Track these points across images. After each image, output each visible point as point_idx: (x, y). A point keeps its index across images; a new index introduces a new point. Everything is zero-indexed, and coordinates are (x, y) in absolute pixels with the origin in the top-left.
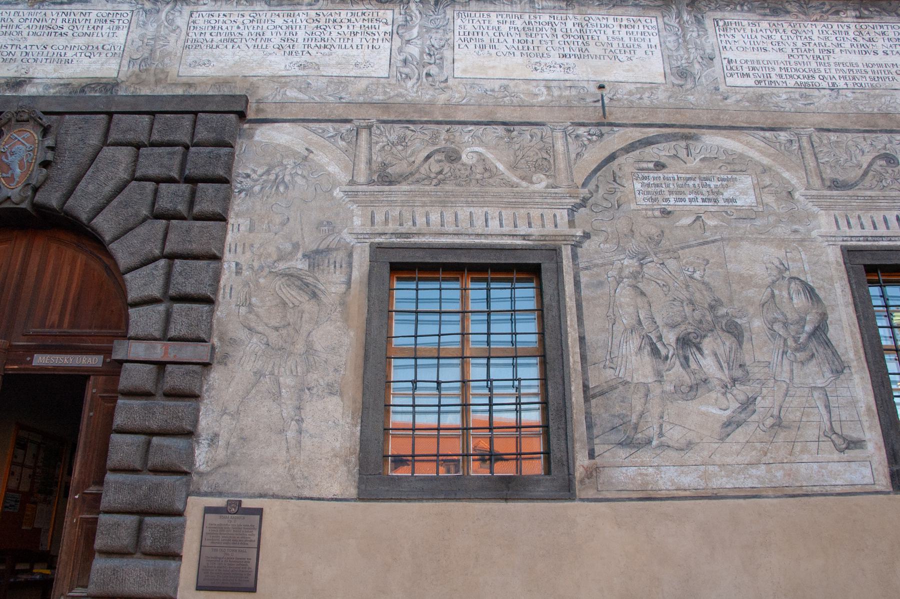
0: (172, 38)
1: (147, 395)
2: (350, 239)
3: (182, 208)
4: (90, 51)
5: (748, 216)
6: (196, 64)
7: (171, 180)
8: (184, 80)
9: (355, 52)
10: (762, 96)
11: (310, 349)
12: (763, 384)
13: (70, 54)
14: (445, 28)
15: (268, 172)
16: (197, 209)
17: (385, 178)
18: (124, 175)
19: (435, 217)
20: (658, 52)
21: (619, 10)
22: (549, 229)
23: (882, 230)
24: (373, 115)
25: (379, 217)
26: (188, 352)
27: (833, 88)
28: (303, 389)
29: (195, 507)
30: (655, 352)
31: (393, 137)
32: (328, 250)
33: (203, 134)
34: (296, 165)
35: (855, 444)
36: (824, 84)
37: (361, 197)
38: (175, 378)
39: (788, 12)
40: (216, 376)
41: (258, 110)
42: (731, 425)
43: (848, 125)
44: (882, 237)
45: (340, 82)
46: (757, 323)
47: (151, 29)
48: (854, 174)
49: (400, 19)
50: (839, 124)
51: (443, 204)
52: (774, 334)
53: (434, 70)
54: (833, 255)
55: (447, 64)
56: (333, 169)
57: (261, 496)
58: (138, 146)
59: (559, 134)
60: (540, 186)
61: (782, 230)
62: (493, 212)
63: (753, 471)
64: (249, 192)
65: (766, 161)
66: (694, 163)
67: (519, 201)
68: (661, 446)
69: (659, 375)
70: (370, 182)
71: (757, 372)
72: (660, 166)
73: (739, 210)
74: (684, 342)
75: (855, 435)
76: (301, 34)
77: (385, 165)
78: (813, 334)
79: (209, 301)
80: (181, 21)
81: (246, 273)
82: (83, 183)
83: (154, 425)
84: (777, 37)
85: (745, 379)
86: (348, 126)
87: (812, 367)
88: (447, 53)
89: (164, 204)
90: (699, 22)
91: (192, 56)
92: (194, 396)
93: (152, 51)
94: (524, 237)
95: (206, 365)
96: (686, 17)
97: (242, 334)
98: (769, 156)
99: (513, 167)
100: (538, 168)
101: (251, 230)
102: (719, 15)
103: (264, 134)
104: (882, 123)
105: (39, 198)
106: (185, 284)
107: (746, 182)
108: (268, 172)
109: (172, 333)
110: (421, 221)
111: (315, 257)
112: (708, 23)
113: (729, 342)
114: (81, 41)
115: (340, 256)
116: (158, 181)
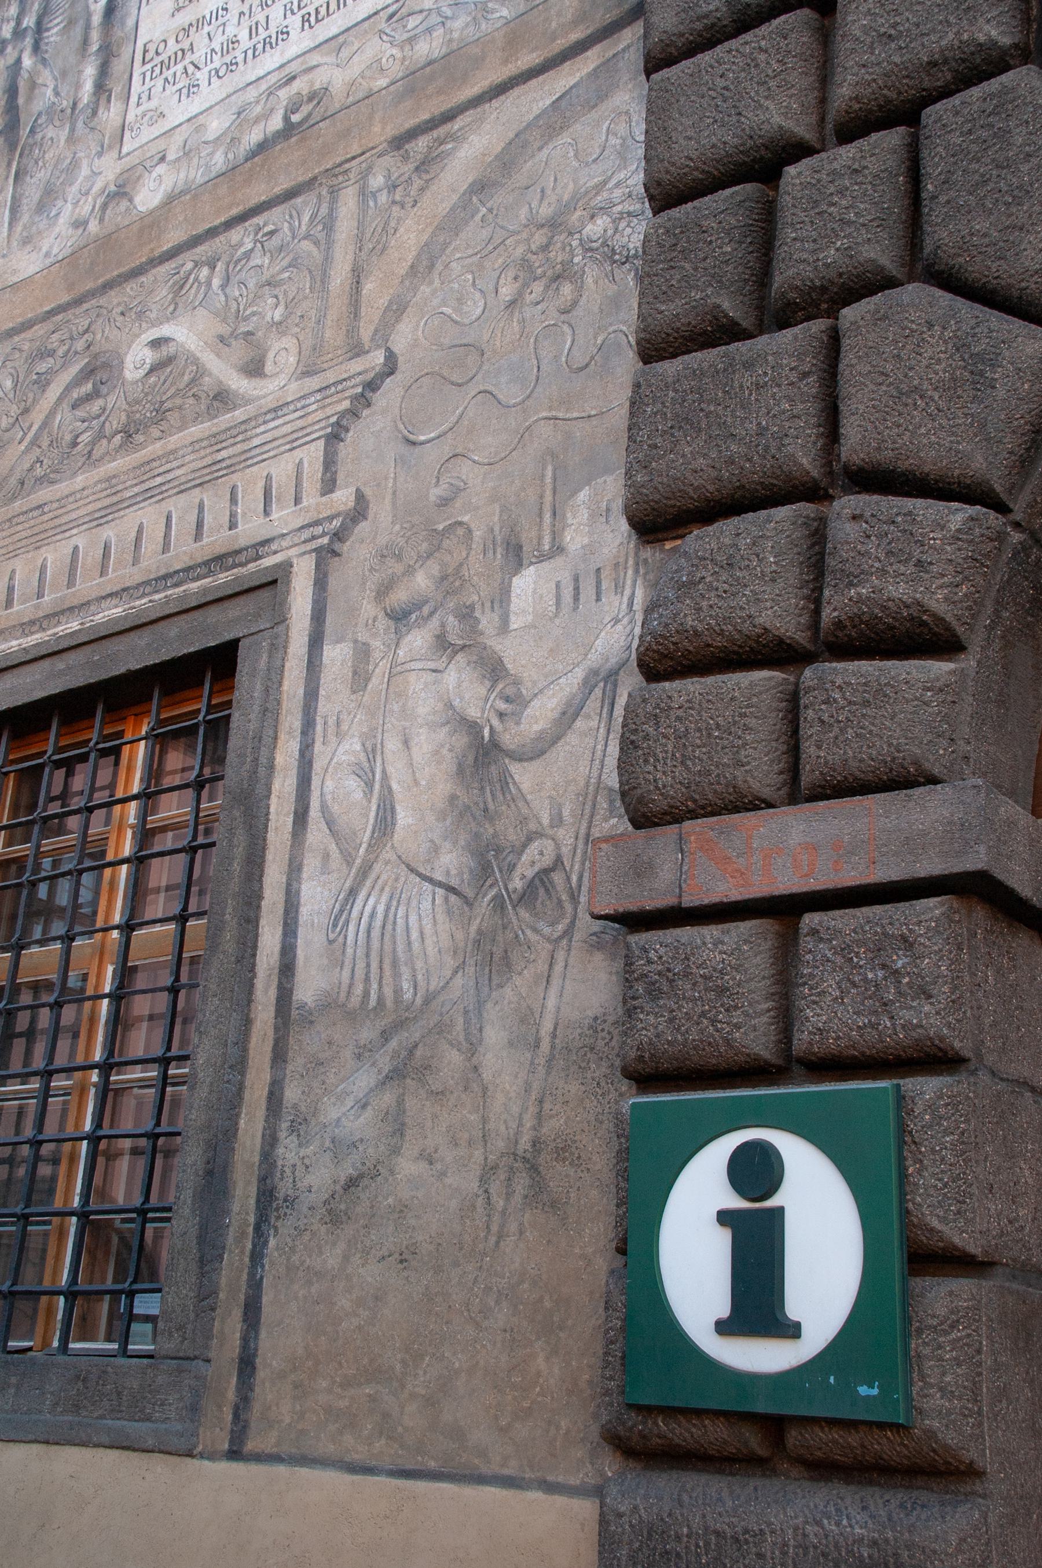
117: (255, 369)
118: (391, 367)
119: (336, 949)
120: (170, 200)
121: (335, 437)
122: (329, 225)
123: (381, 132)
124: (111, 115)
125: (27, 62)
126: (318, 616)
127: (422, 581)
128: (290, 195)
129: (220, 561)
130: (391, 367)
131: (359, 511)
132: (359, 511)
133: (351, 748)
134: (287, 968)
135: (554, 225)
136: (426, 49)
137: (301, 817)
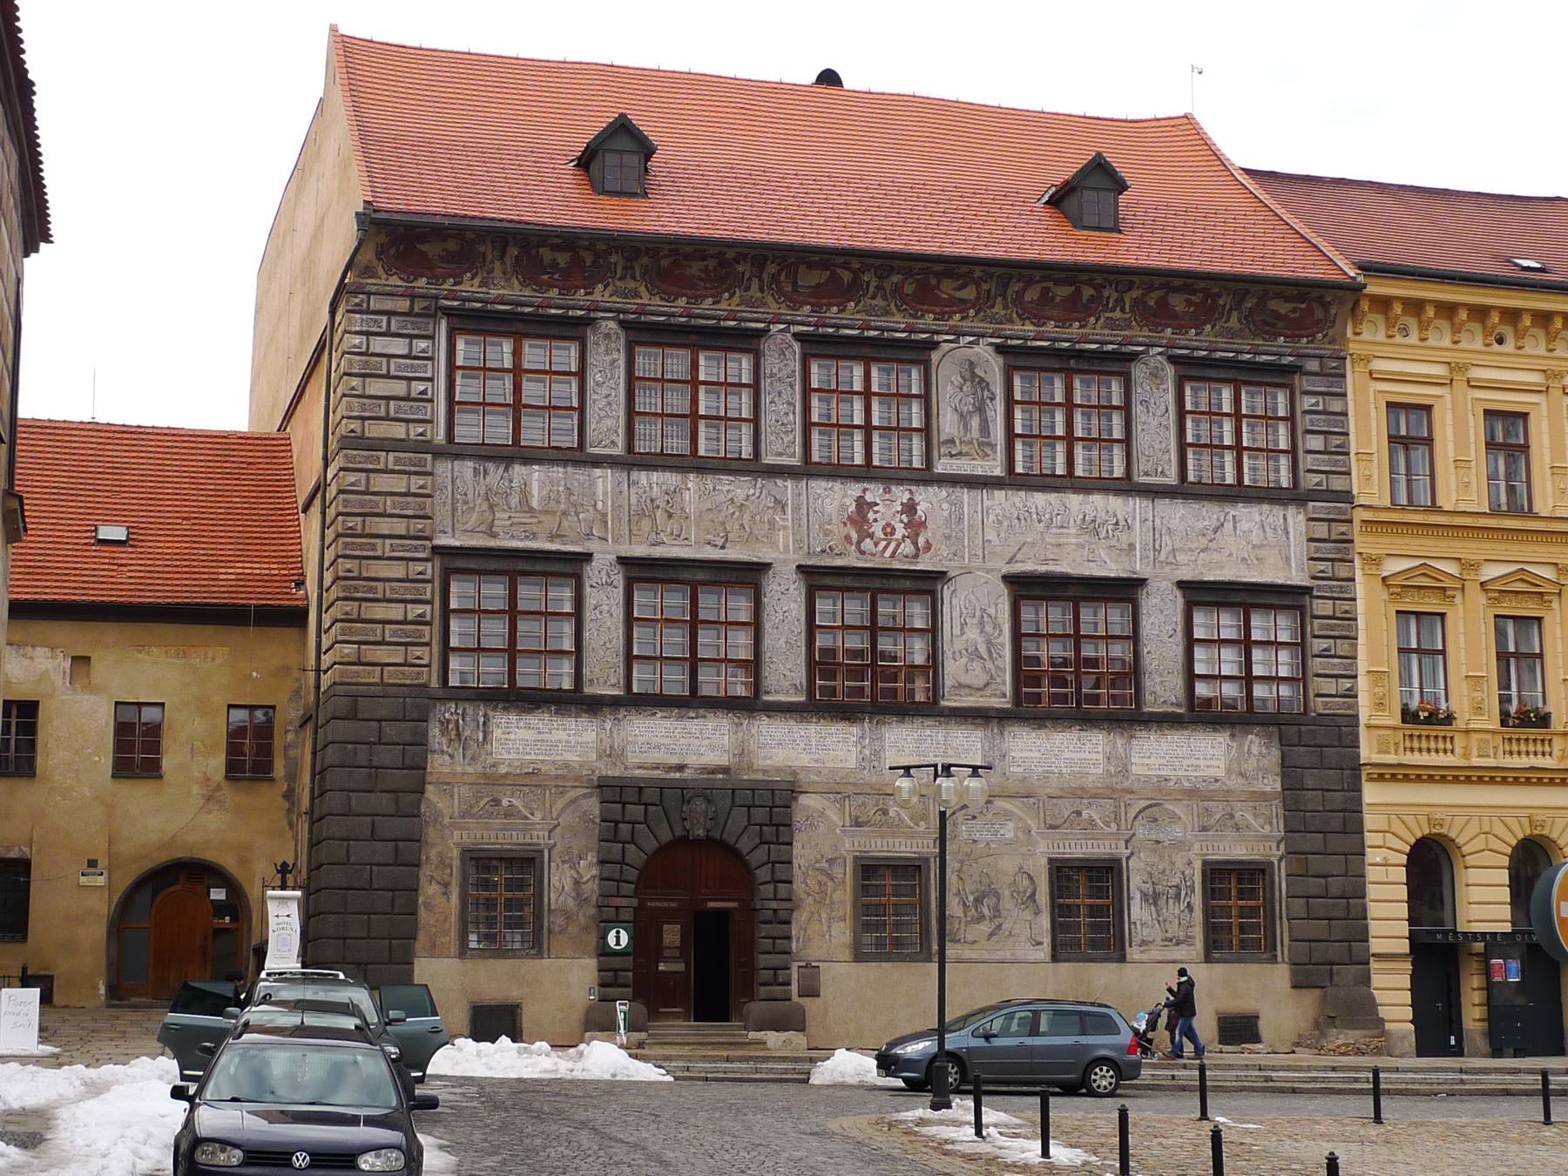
0: (752, 743)
1: (770, 923)
2: (844, 853)
3: (775, 840)
4: (713, 748)
5: (1009, 843)
6: (765, 758)
7: (767, 825)
8: (760, 768)
9: (840, 753)
10: (1025, 778)
11: (832, 903)
12: (1005, 918)
13: (703, 750)
14: (881, 739)
15: (807, 820)
16: (781, 841)
17: (857, 823)
18: (746, 823)
19: (879, 843)
20: (980, 752)
21: (964, 727)
22: (925, 850)
23: (1067, 850)
24: (850, 790)
25: (856, 844)
26: (786, 905)
27: (1061, 773)
28: (830, 919)
29: (795, 966)
30: (964, 904)
31: (860, 802)
32: (836, 858)
33: (778, 802)
34: (819, 817)
35: (1040, 943)
36: (1056, 771)
37: (847, 833)
38: (782, 915)
39: (1046, 727)
40: (795, 914)
41: (800, 787)
42: (992, 935)
43: (1063, 795)
44: (1066, 853)
45: (834, 771)
46: (1007, 892)
47: (741, 734)
48: (1059, 822)
49: (860, 732)
50: (1059, 794)
51: (882, 837)
52: (1013, 897)
53: (876, 764)
54: (1044, 862)
55: (882, 760)
56: (835, 819)
57: (819, 961)
58: (749, 807)
59: (931, 801)
60: (922, 829)
61: (1024, 850)
62: (903, 841)
63: (999, 953)
64: (800, 830)
65: (1021, 814)
66: (990, 816)
67: (913, 835)
68: (965, 942)
69: (966, 916)
70: (851, 826)
71: (1004, 913)
72: (974, 817)
73: (1005, 839)
74: (976, 900)
75: (1041, 940)
76: (814, 743)
77: (857, 817)
78: (1029, 898)
79: (790, 882)
80: (754, 731)
81: (803, 868)
82: (728, 826)
83: (775, 935)
84: (1038, 742)
85: (1000, 916)
86: (840, 796)
87: (1027, 911)
88: (882, 754)
89: (767, 837)
90: (1002, 733)
91: (762, 753)
92: (789, 923)
93: (743, 749)
94: (915, 853)
95: (792, 910)
96: (996, 731)
97: (805, 896)
98: (1024, 811)
99: (911, 819)
100: (922, 819)
101: (803, 848)
102: (1011, 729)
103: (804, 800)
104: (1079, 792)
105: (710, 834)
106: (780, 876)
107: (1011, 825)
108: (807, 820)
109: (779, 897)
110: (873, 845)
111: (831, 861)
112: (1006, 733)
113: (994, 900)
114: (706, 742)
115: (842, 860)
116: (761, 825)
117: (532, 814)
118: (559, 824)
119: (557, 903)
120: (507, 773)
121: (550, 832)
122: (545, 794)
123: (553, 783)
124: (489, 746)
125: (461, 721)
126: (549, 857)
127: (567, 858)
128: (536, 786)
129: (529, 845)
130: (559, 824)
131: (555, 844)
132: (555, 844)
133: (557, 878)
134: (549, 904)
135: (585, 812)
136: (559, 772)
137: (549, 885)
